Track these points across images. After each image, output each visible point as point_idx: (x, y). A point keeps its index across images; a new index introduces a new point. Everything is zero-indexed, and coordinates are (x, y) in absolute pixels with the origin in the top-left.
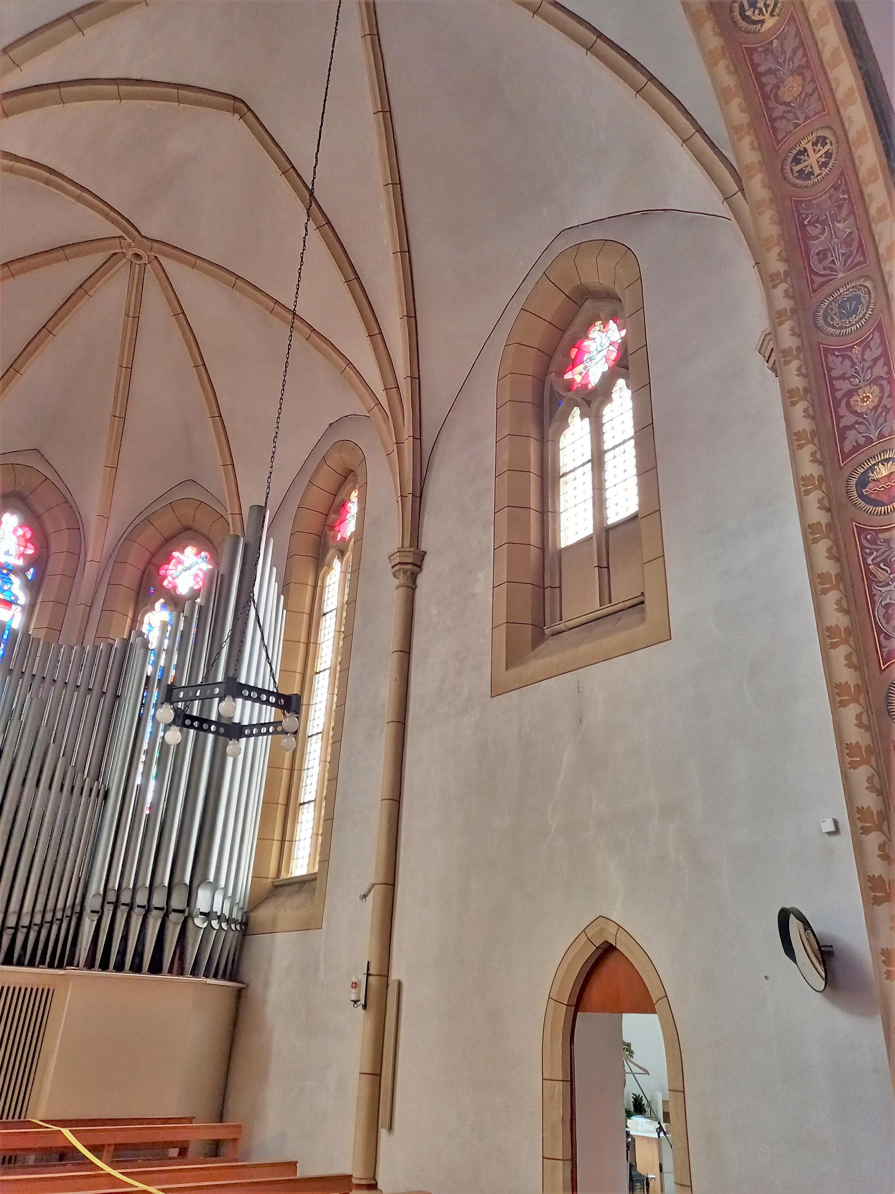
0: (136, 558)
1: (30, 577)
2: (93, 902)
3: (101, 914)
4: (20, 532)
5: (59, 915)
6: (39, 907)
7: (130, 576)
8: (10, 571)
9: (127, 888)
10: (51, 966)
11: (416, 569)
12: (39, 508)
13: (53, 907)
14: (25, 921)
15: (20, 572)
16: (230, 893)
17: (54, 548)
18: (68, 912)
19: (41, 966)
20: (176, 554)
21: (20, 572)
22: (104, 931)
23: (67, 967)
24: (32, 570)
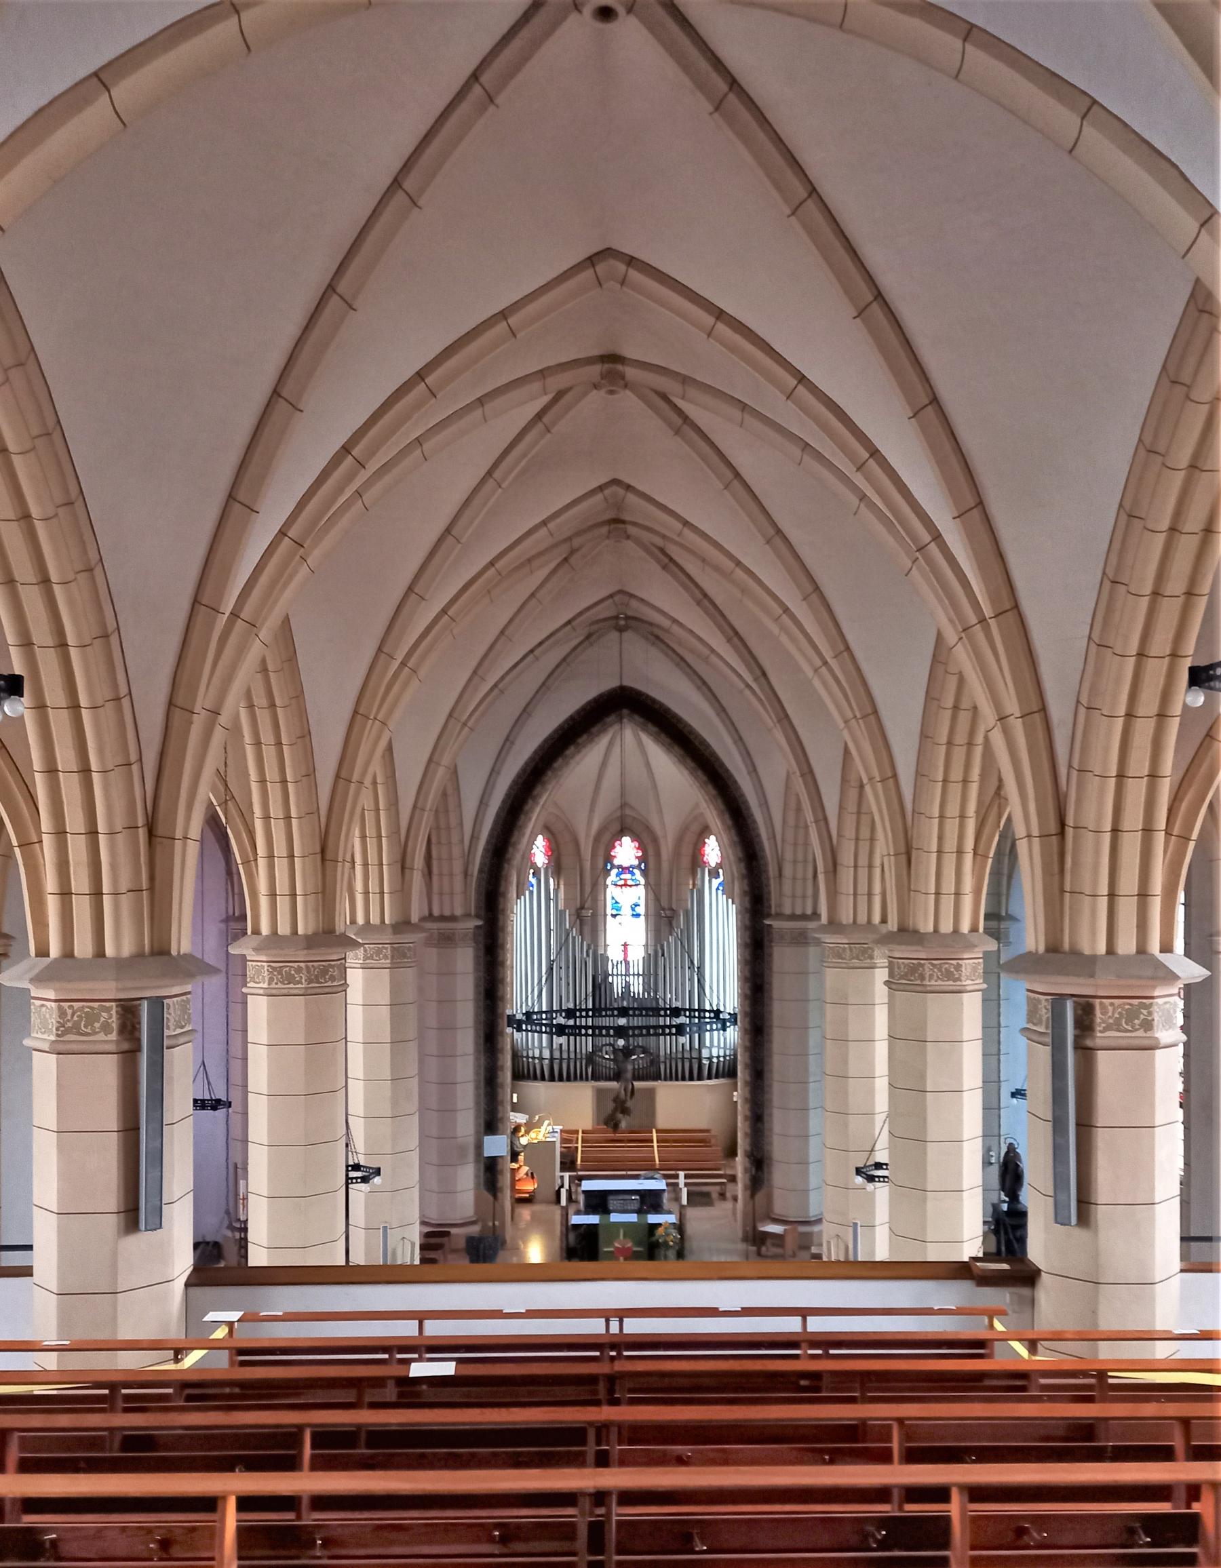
0: (687, 851)
3: (665, 1063)
7: (686, 861)
15: (639, 867)
16: (722, 1045)
20: (706, 840)
21: (639, 867)
24: (643, 864)
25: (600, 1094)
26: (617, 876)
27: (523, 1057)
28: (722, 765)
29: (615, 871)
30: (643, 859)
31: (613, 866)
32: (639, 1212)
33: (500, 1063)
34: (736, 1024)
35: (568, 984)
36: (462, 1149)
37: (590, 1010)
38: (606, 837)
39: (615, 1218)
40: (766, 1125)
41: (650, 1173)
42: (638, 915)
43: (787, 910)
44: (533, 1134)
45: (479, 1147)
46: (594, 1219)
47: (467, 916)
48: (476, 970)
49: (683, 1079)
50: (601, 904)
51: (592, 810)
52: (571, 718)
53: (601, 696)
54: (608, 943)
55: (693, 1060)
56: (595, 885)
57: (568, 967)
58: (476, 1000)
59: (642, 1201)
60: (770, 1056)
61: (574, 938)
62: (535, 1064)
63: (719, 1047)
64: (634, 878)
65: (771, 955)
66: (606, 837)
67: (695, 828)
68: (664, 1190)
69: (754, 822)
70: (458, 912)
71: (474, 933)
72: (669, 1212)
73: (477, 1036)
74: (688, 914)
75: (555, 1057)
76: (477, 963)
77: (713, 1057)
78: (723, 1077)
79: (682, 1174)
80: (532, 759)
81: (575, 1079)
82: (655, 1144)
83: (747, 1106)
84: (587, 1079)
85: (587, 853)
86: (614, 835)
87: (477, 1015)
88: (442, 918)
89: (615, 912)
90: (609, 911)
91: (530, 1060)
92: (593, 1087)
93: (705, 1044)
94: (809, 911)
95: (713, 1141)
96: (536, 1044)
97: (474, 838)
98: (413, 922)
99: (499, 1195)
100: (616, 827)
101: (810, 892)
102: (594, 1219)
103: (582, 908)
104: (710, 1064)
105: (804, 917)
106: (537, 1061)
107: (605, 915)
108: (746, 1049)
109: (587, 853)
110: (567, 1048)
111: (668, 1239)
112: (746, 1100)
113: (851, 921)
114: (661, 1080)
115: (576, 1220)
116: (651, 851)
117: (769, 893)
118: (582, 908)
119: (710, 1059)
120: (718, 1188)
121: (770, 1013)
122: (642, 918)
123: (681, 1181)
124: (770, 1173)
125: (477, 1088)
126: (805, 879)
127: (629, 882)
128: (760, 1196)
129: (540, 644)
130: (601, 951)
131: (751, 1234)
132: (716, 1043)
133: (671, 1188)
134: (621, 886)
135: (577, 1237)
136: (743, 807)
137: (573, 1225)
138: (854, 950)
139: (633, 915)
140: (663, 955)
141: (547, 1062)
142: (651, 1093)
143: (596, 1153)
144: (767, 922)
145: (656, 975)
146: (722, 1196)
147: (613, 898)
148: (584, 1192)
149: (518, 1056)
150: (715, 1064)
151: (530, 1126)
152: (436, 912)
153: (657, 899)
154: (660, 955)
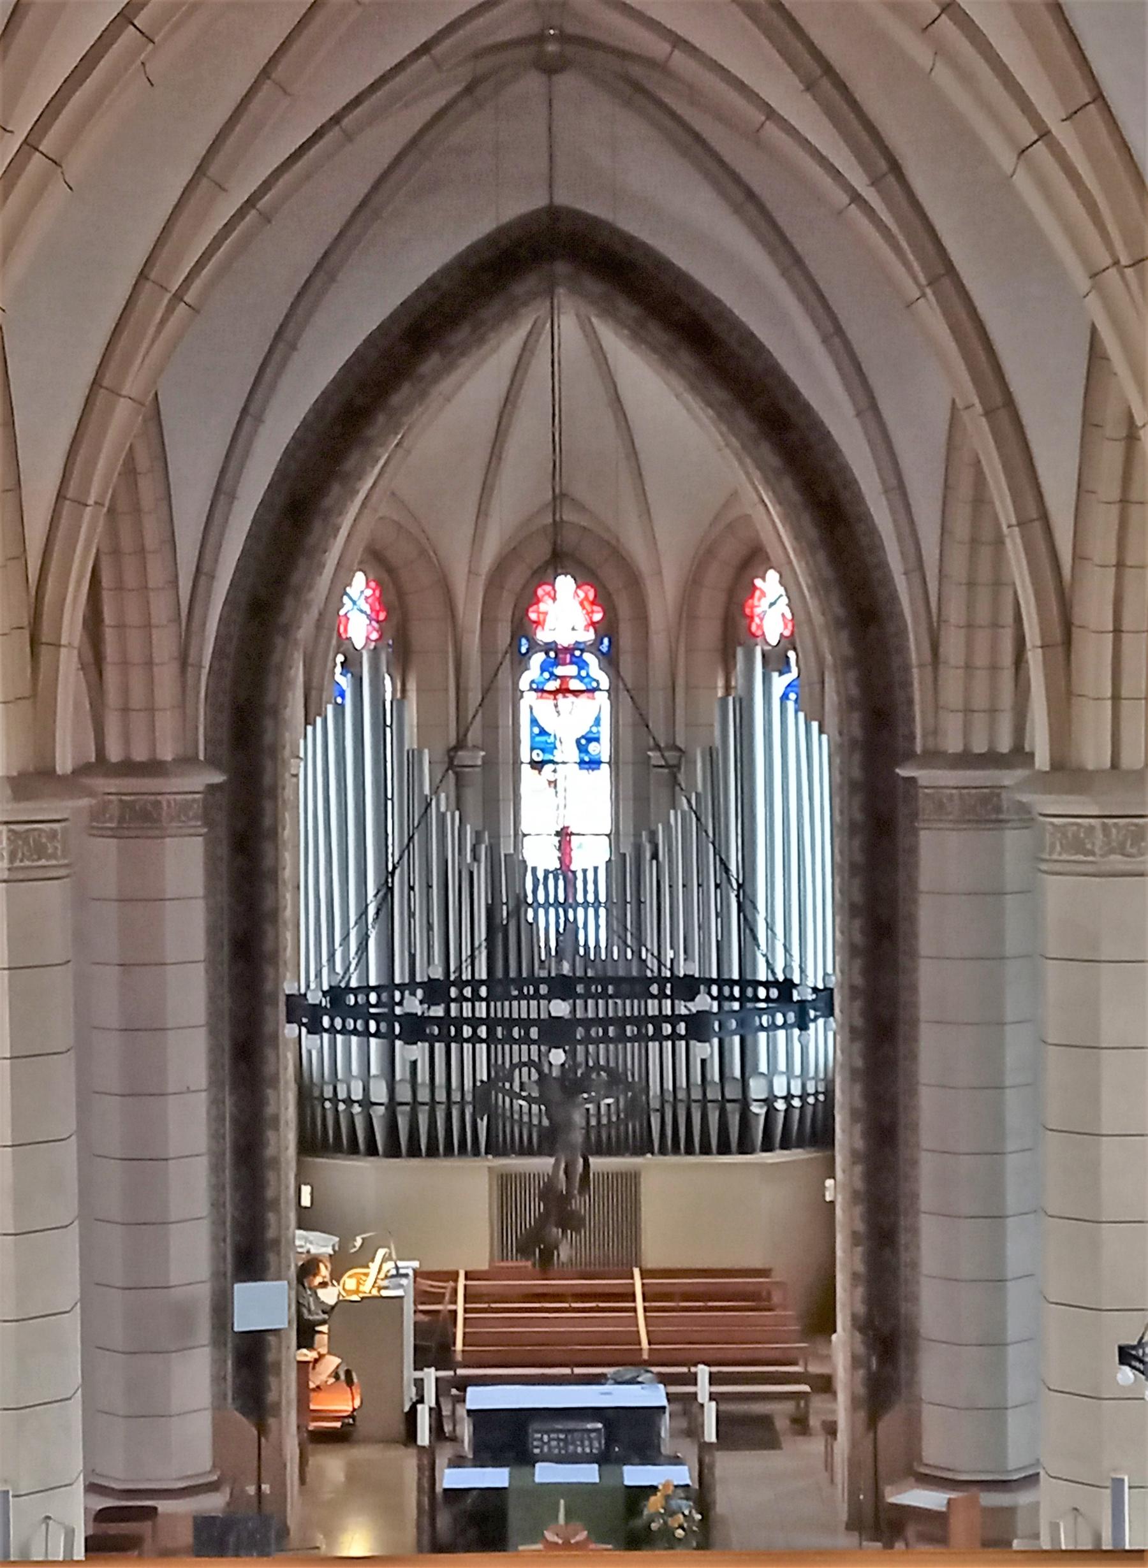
0: (710, 605)
2: (655, 1104)
4: (582, 594)
7: (708, 633)
8: (582, 651)
9: (681, 1088)
15: (594, 647)
16: (797, 1070)
20: (758, 582)
21: (594, 647)
24: (606, 641)
25: (505, 1184)
26: (543, 670)
28: (794, 394)
29: (538, 659)
30: (606, 629)
31: (534, 647)
32: (603, 1459)
33: (270, 1110)
34: (832, 1014)
35: (430, 927)
36: (183, 1316)
37: (482, 982)
38: (516, 578)
39: (546, 1473)
40: (905, 1257)
41: (629, 1372)
42: (592, 764)
43: (953, 744)
44: (349, 1282)
45: (222, 1308)
46: (496, 1477)
47: (187, 761)
48: (210, 892)
49: (706, 1150)
50: (504, 734)
51: (482, 512)
52: (431, 284)
53: (502, 231)
54: (524, 827)
55: (729, 1106)
56: (488, 690)
57: (430, 887)
58: (212, 963)
59: (610, 1439)
60: (913, 1092)
61: (442, 817)
62: (351, 1116)
64: (583, 673)
65: (913, 850)
66: (516, 578)
67: (731, 551)
68: (664, 1408)
69: (873, 531)
70: (167, 754)
71: (205, 800)
72: (676, 1461)
73: (214, 1050)
74: (712, 757)
75: (399, 1099)
76: (211, 873)
77: (776, 1098)
78: (799, 1146)
79: (703, 1372)
80: (337, 383)
81: (449, 1151)
82: (640, 1303)
83: (859, 1210)
84: (476, 1153)
85: (471, 616)
86: (535, 573)
87: (212, 998)
88: (129, 768)
89: (538, 756)
90: (525, 755)
91: (342, 1106)
94: (1005, 745)
95: (776, 1298)
97: (202, 573)
98: (59, 771)
99: (271, 1421)
101: (1007, 697)
102: (496, 1477)
103: (460, 745)
104: (767, 1113)
105: (992, 759)
106: (357, 1109)
107: (517, 763)
108: (854, 1074)
109: (471, 616)
110: (427, 1081)
111: (673, 1522)
112: (855, 1197)
113: (1108, 764)
115: (452, 1478)
117: (910, 702)
118: (460, 745)
119: (769, 1101)
120: (789, 1407)
121: (913, 988)
122: (605, 768)
123: (703, 1389)
124: (913, 1368)
125: (216, 1169)
126: (994, 668)
127: (575, 685)
128: (889, 1423)
129: (357, 101)
130: (506, 848)
131: (868, 1510)
132: (782, 1066)
133: (678, 1407)
134: (554, 693)
135: (455, 1520)
136: (845, 496)
137: (446, 1490)
138: (1114, 831)
139: (582, 763)
140: (655, 856)
141: (381, 1110)
142: (631, 1181)
143: (497, 1320)
144: (903, 772)
146: (800, 1424)
147: (534, 722)
148: (469, 1412)
149: (311, 1098)
150: (781, 1115)
151: (341, 1263)
152: (114, 754)
153: (642, 722)
154: (648, 856)
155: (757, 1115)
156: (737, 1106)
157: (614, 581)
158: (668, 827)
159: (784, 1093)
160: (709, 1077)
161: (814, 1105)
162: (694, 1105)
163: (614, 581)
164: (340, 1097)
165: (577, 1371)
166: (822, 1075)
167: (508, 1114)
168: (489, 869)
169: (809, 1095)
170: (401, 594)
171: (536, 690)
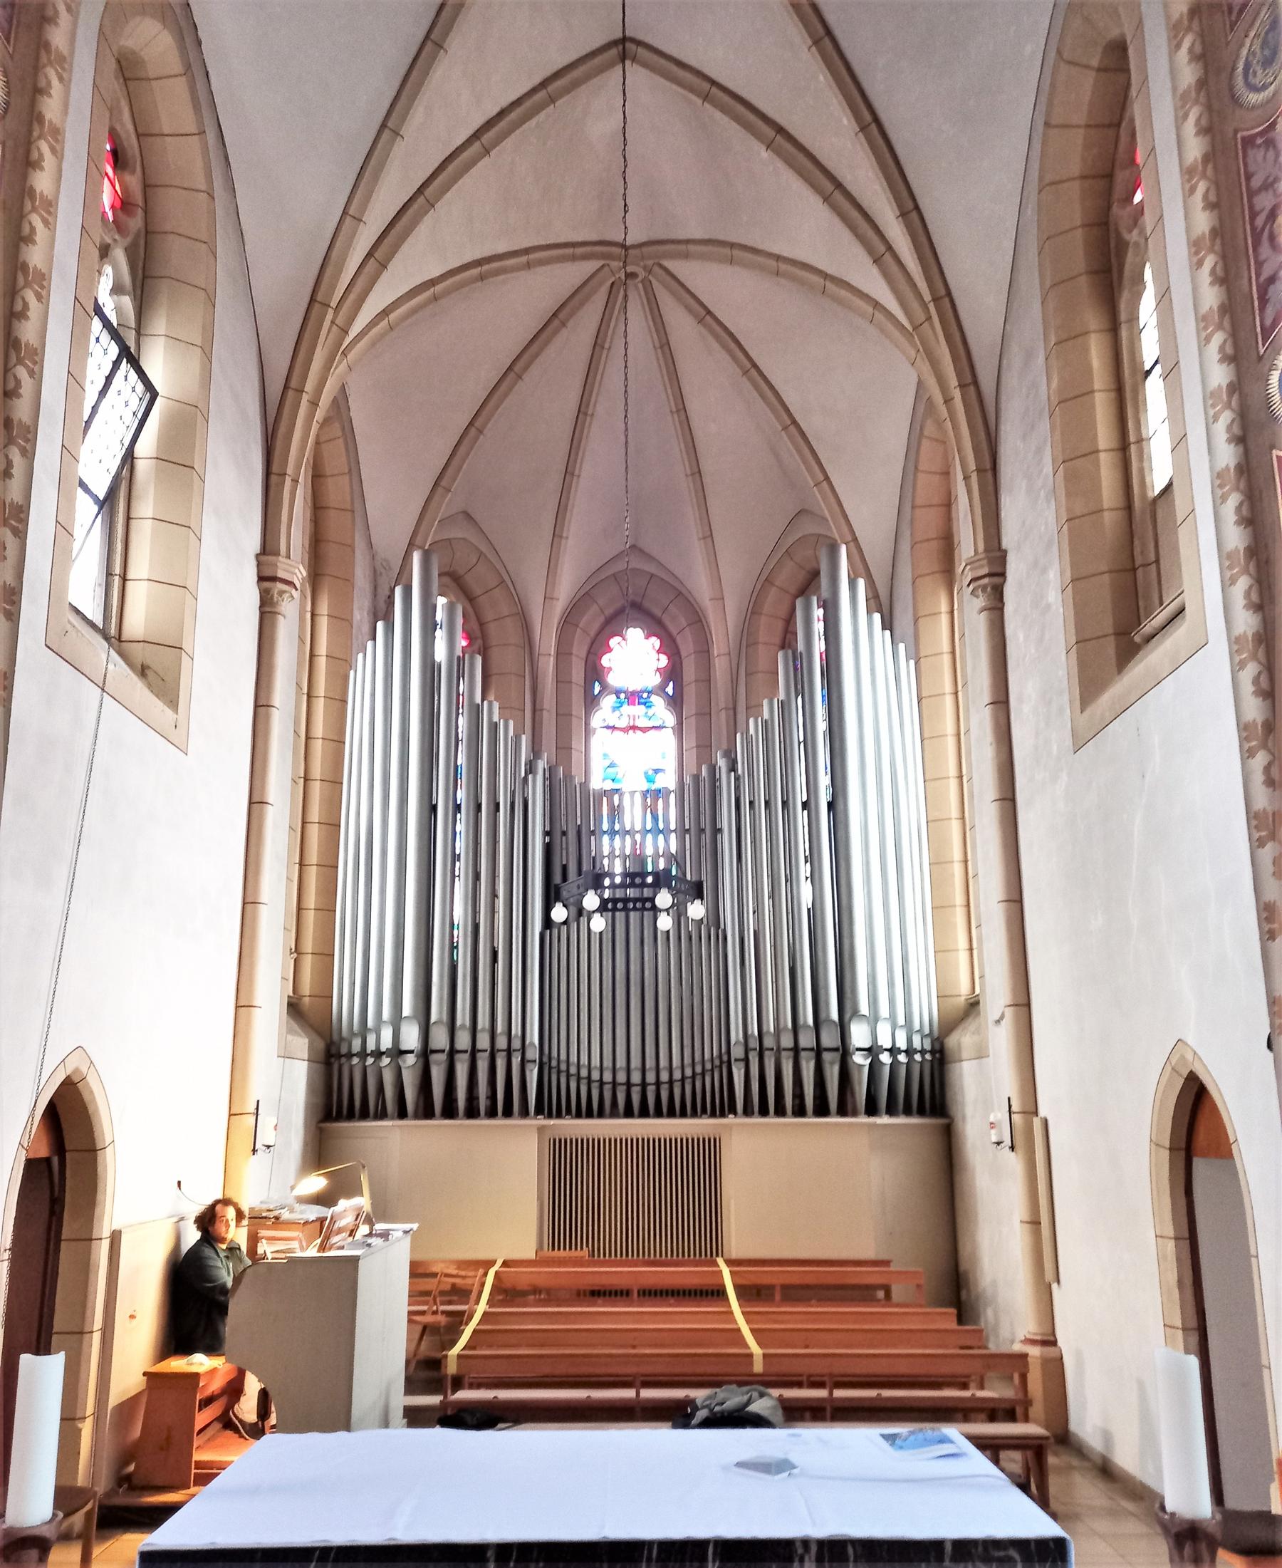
1: (671, 693)
2: (737, 1052)
3: (746, 1061)
5: (708, 1066)
6: (687, 1060)
9: (768, 1032)
10: (713, 1115)
11: (997, 580)
12: (657, 612)
13: (710, 1057)
14: (677, 1075)
16: (901, 1021)
17: (683, 654)
18: (717, 1062)
19: (703, 1116)
21: (661, 689)
22: (755, 1077)
23: (730, 1116)
24: (671, 683)
26: (614, 709)
27: (350, 1055)
30: (673, 673)
38: (591, 620)
56: (563, 716)
61: (494, 727)
63: (893, 1017)
66: (591, 620)
78: (908, 1112)
84: (525, 1113)
85: (547, 642)
86: (608, 621)
92: (541, 1129)
93: (855, 1012)
96: (386, 1014)
100: (608, 600)
104: (871, 1064)
109: (547, 642)
110: (468, 1023)
114: (735, 1113)
116: (687, 646)
119: (873, 1051)
127: (642, 723)
140: (733, 768)
141: (410, 1060)
142: (710, 1150)
145: (717, 831)
150: (887, 1069)
155: (861, 1066)
156: (836, 1056)
157: (677, 621)
158: (748, 740)
159: (889, 1046)
160: (801, 1021)
161: (921, 1063)
162: (784, 1054)
163: (677, 621)
164: (369, 1051)
165: (648, 1394)
166: (927, 1031)
167: (563, 1067)
168: (548, 797)
169: (916, 1051)
170: (482, 625)
171: (608, 727)
